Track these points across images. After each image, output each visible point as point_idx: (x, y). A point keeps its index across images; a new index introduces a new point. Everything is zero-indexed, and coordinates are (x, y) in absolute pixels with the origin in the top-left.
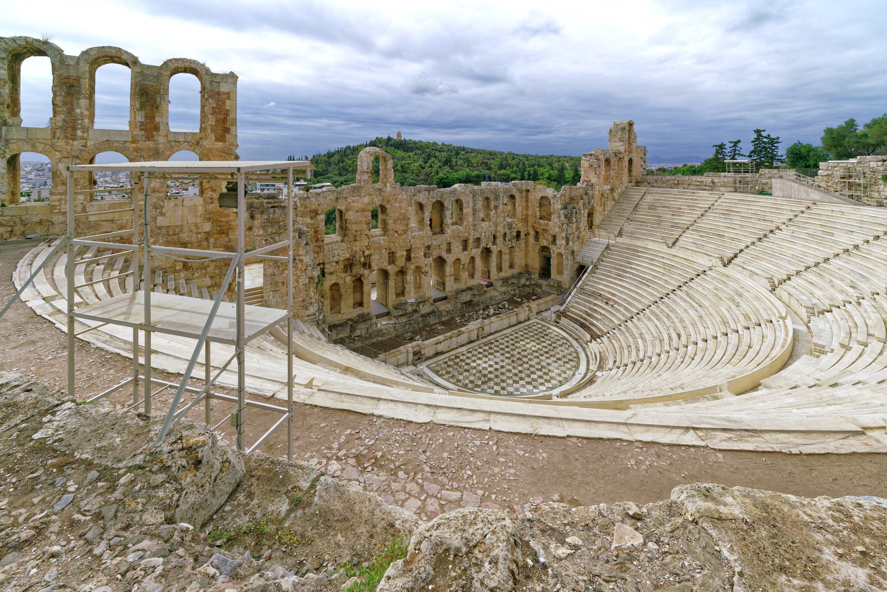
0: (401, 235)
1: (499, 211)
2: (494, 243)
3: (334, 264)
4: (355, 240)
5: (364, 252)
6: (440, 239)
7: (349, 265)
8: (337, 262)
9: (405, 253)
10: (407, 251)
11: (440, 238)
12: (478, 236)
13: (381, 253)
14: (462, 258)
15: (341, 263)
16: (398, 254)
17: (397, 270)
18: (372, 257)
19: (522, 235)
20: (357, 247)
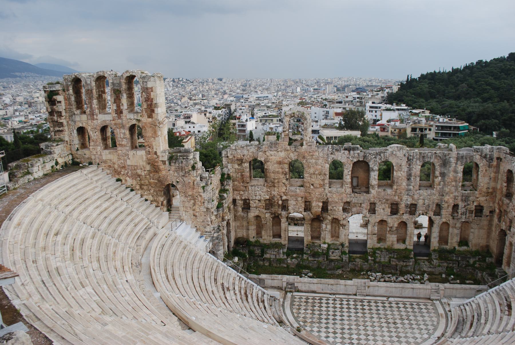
0: (316, 188)
2: (438, 213)
3: (257, 202)
4: (274, 186)
5: (281, 197)
6: (362, 198)
7: (269, 204)
8: (259, 201)
9: (321, 204)
10: (323, 202)
11: (363, 197)
12: (414, 202)
13: (297, 200)
15: (263, 202)
16: (314, 204)
17: (312, 217)
18: (289, 202)
19: (486, 212)
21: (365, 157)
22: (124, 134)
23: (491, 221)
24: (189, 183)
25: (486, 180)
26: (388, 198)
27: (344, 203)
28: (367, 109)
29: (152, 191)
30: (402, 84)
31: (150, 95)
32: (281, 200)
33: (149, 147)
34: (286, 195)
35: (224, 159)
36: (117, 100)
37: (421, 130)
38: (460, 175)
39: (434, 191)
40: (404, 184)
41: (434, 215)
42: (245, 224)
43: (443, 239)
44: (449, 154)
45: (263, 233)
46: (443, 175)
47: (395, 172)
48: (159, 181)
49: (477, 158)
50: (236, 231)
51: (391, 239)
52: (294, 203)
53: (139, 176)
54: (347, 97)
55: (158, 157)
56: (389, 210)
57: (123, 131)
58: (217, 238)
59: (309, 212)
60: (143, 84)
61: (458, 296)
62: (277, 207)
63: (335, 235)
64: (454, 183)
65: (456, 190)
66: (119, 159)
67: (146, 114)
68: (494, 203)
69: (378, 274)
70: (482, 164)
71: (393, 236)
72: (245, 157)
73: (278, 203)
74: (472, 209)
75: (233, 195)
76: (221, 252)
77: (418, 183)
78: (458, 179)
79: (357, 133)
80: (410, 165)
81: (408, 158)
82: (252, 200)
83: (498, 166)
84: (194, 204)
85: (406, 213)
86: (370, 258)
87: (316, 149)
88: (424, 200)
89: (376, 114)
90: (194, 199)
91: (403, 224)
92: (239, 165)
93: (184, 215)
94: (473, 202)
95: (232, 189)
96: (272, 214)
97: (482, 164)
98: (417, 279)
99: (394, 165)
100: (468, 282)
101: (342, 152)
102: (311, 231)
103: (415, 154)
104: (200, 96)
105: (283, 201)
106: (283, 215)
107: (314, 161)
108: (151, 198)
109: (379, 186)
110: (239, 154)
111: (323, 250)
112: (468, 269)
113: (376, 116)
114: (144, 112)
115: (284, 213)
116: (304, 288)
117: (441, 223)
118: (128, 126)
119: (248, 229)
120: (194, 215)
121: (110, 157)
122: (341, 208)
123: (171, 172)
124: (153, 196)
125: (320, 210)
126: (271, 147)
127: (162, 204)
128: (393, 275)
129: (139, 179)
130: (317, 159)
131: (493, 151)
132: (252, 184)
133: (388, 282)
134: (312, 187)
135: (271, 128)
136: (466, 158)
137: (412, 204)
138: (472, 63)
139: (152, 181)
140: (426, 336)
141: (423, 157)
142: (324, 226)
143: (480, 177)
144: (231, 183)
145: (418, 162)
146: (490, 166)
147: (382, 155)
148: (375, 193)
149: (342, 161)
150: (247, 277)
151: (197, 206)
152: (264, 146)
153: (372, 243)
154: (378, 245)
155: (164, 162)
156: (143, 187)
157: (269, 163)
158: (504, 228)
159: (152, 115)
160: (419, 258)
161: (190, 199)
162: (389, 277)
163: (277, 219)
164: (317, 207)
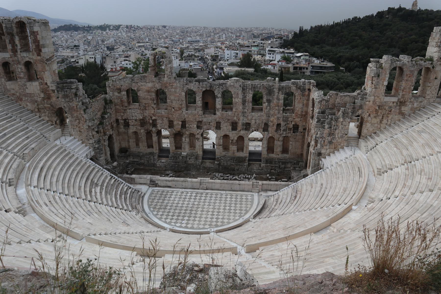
0: (176, 110)
1: (271, 104)
3: (134, 121)
4: (146, 109)
5: (151, 117)
6: (210, 118)
7: (143, 122)
8: (136, 120)
9: (180, 123)
12: (248, 122)
13: (163, 120)
14: (231, 135)
16: (175, 123)
18: (157, 121)
19: (300, 129)
20: (147, 113)
21: (211, 87)
22: (21, 68)
23: (304, 136)
24: (73, 106)
25: (301, 105)
26: (230, 118)
27: (198, 122)
28: (267, 52)
29: (47, 113)
30: (295, 33)
31: (37, 37)
32: (152, 119)
33: (41, 79)
34: (154, 116)
35: (108, 89)
36: (12, 42)
37: (301, 68)
38: (282, 102)
39: (262, 113)
40: (241, 108)
41: (263, 131)
42: (126, 137)
43: (270, 149)
44: (273, 85)
45: (140, 144)
46: (269, 101)
47: (233, 99)
48: (52, 106)
49: (293, 88)
50: (120, 143)
51: (233, 149)
52: (161, 122)
53: (36, 101)
54: (254, 42)
55: (49, 87)
56: (231, 127)
57: (20, 66)
58: (98, 148)
59: (172, 129)
60: (30, 28)
61: (272, 189)
62: (148, 125)
63: (192, 146)
64: (277, 108)
65: (279, 113)
66: (20, 89)
67: (36, 53)
68: (306, 123)
69: (220, 174)
70: (297, 93)
71: (234, 146)
72: (123, 87)
73: (149, 122)
74: (290, 127)
75: (116, 116)
76: (102, 159)
77: (251, 108)
78: (280, 104)
79: (251, 70)
80: (244, 93)
81: (243, 88)
82: (130, 120)
83: (309, 95)
84: (79, 123)
85: (243, 129)
86: (216, 162)
87: (175, 81)
88: (256, 120)
89: (274, 56)
90: (79, 119)
91: (241, 138)
92: (119, 93)
93: (72, 131)
94: (291, 122)
95: (114, 112)
96: (145, 130)
97: (297, 94)
98: (248, 178)
99: (233, 93)
100: (283, 180)
101: (194, 83)
102: (175, 142)
103: (248, 86)
104: (147, 40)
105: (153, 120)
106: (153, 131)
107: (173, 90)
108: (47, 119)
109: (223, 109)
110: (118, 84)
111: (183, 157)
112: (286, 171)
113: (273, 57)
114: (34, 51)
115: (154, 129)
116: (162, 185)
117: (268, 137)
118: (23, 62)
119: (129, 142)
120: (80, 131)
121: (12, 87)
122: (195, 126)
123: (59, 98)
124: (48, 117)
125: (180, 127)
126: (141, 79)
127: (56, 123)
128: (231, 174)
129: (36, 104)
130: (176, 88)
131: (305, 84)
132: (130, 108)
133: (225, 180)
134: (173, 110)
135: (191, 66)
136: (286, 89)
137: (247, 123)
138: (349, 19)
139: (46, 105)
140: (237, 218)
141: (254, 87)
142: (184, 139)
143: (296, 103)
144: (113, 106)
145: (250, 91)
146: (303, 95)
147: (224, 85)
148: (219, 115)
149: (194, 90)
150: (118, 177)
151: (81, 124)
152: (136, 79)
153: (219, 152)
154: (224, 153)
155: (53, 91)
156: (40, 110)
157: (141, 91)
158: (309, 141)
159: (40, 54)
160: (253, 162)
161: (76, 120)
162: (228, 177)
163: (149, 134)
164: (178, 125)
